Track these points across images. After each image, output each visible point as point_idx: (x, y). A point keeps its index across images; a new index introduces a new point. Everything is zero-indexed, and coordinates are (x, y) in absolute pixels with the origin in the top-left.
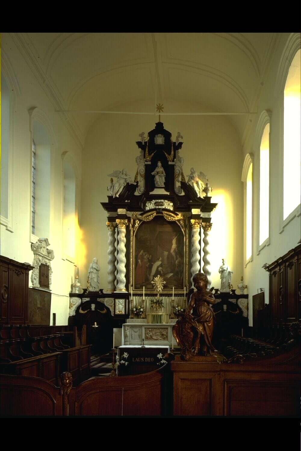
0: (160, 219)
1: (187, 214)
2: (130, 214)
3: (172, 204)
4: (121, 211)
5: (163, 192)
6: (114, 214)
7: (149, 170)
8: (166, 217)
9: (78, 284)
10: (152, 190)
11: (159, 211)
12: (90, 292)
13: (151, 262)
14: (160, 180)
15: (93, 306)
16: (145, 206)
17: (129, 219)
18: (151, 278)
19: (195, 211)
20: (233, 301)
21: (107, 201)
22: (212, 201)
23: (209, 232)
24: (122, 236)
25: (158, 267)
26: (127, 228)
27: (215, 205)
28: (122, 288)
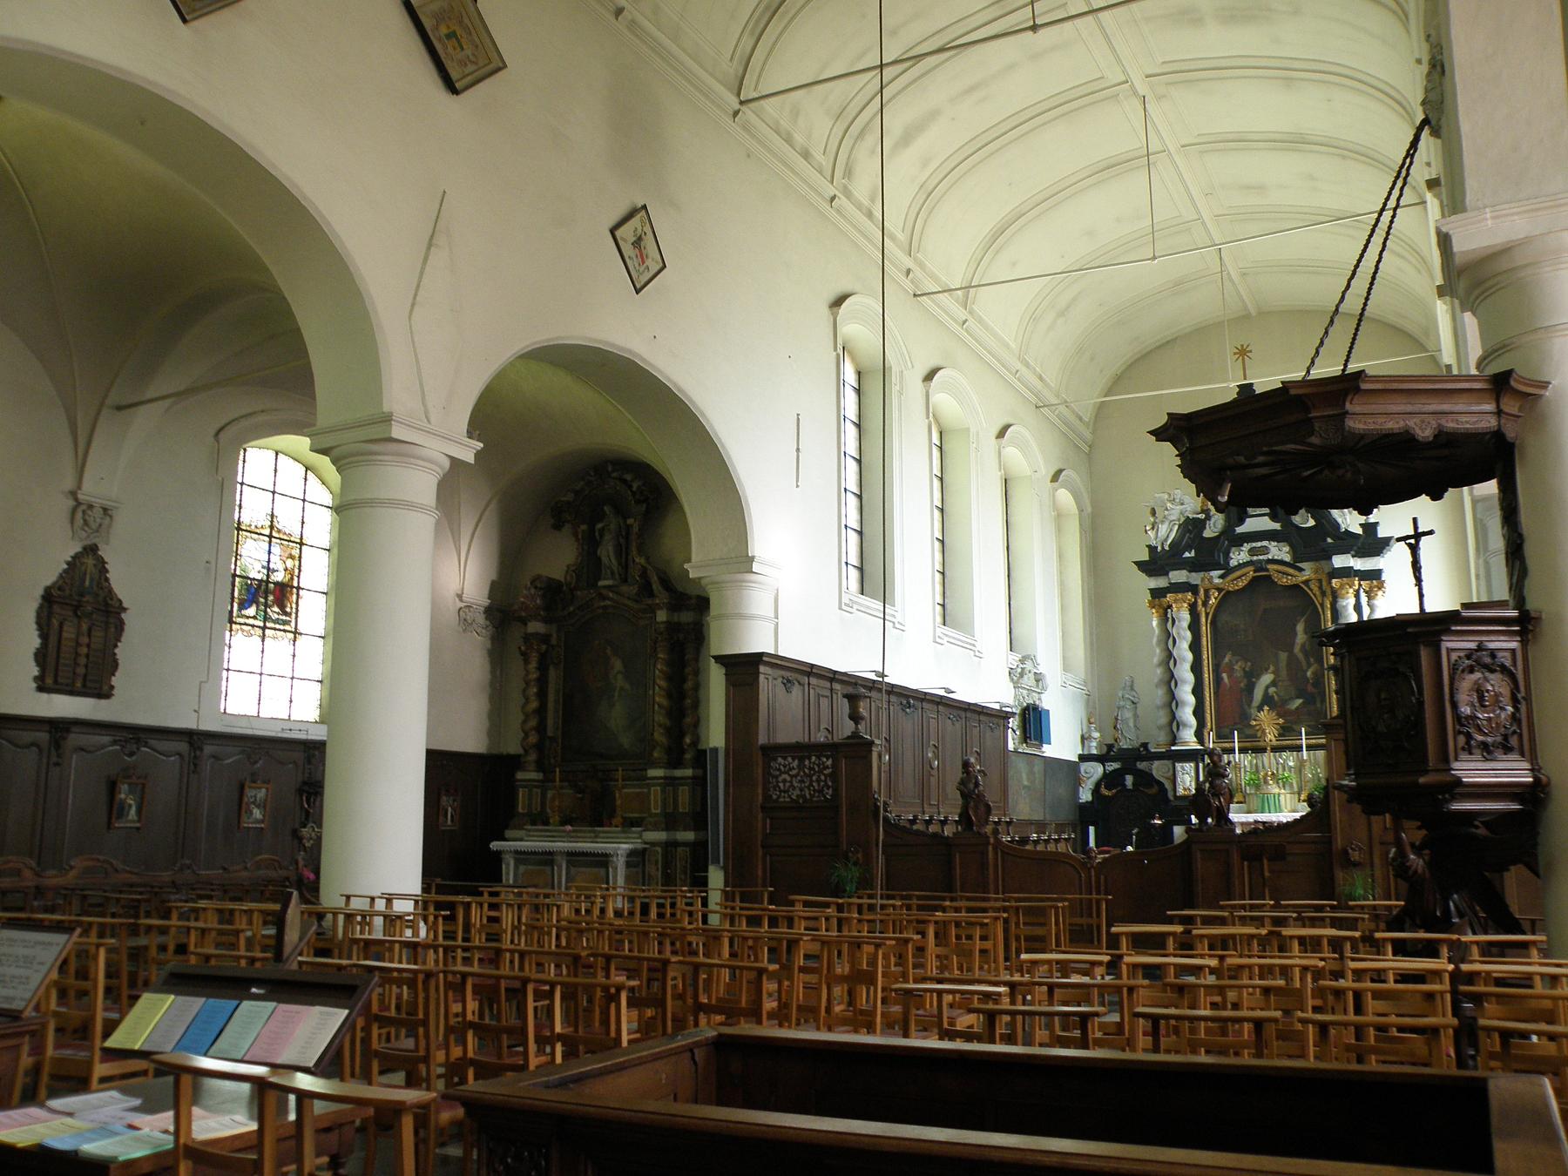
0: (1262, 581)
2: (1195, 578)
3: (1287, 549)
4: (1179, 576)
6: (1160, 582)
8: (1276, 577)
9: (1096, 735)
10: (1241, 521)
11: (1259, 566)
12: (1121, 750)
13: (1251, 677)
15: (1129, 780)
16: (1227, 558)
17: (1194, 589)
18: (1253, 711)
19: (1339, 561)
21: (1145, 557)
23: (1376, 602)
25: (1267, 687)
26: (1193, 609)
28: (1189, 740)
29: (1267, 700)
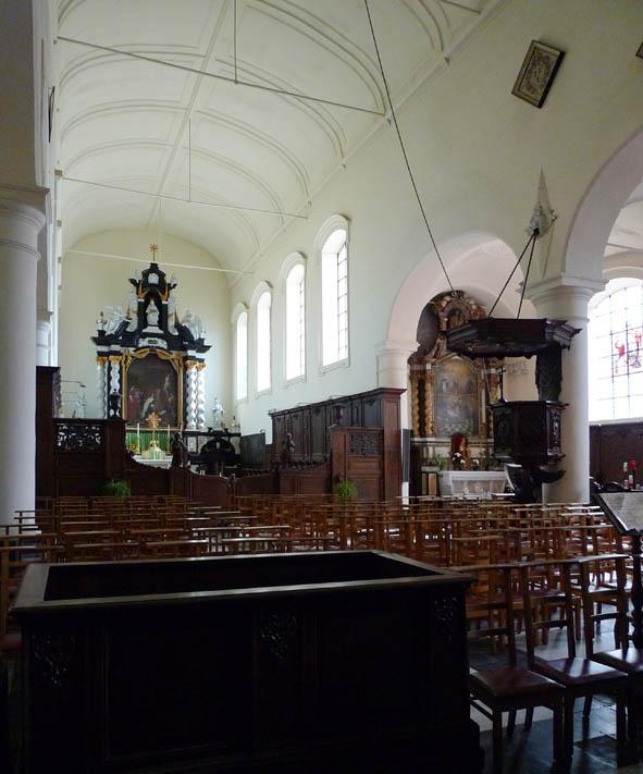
0: (153, 356)
1: (183, 354)
5: (157, 330)
6: (104, 349)
7: (142, 308)
10: (146, 327)
11: (152, 349)
13: (143, 399)
14: (153, 318)
17: (121, 354)
19: (191, 353)
20: (226, 439)
21: (97, 336)
22: (206, 343)
24: (115, 375)
27: (209, 347)
29: (150, 411)
